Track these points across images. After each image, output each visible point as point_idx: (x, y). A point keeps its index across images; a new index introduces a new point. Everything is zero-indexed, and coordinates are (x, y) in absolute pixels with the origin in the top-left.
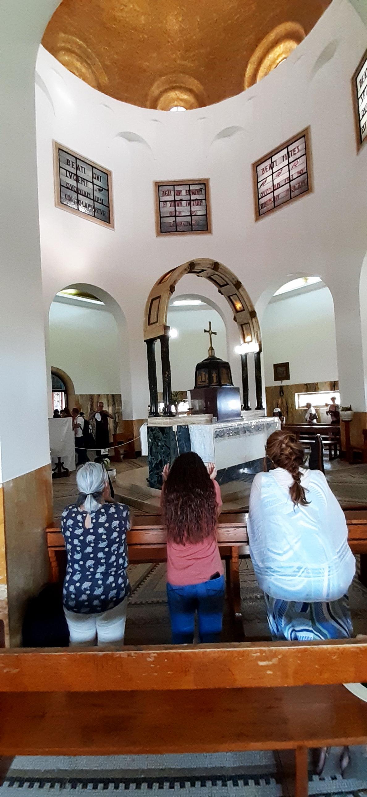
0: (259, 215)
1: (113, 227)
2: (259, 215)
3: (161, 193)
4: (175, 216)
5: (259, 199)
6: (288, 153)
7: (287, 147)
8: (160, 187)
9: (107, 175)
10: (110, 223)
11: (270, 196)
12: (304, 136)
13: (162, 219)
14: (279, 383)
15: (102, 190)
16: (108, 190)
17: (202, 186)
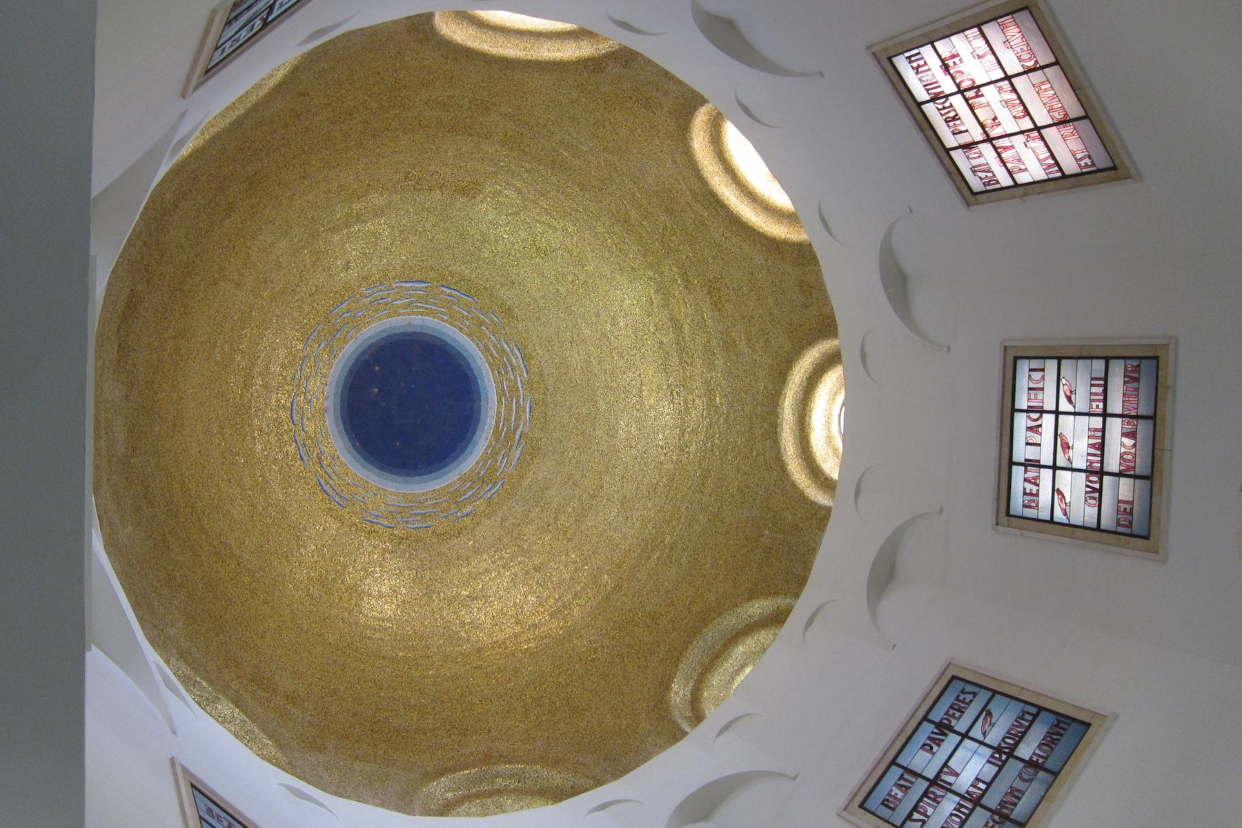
1: (1103, 717)
2: (1114, 168)
3: (1029, 513)
4: (1101, 473)
5: (1064, 176)
6: (933, 100)
7: (919, 105)
8: (1012, 512)
9: (954, 678)
10: (1088, 725)
11: (1052, 134)
12: (890, 59)
13: (1103, 527)
15: (989, 714)
16: (995, 692)
17: (1023, 367)
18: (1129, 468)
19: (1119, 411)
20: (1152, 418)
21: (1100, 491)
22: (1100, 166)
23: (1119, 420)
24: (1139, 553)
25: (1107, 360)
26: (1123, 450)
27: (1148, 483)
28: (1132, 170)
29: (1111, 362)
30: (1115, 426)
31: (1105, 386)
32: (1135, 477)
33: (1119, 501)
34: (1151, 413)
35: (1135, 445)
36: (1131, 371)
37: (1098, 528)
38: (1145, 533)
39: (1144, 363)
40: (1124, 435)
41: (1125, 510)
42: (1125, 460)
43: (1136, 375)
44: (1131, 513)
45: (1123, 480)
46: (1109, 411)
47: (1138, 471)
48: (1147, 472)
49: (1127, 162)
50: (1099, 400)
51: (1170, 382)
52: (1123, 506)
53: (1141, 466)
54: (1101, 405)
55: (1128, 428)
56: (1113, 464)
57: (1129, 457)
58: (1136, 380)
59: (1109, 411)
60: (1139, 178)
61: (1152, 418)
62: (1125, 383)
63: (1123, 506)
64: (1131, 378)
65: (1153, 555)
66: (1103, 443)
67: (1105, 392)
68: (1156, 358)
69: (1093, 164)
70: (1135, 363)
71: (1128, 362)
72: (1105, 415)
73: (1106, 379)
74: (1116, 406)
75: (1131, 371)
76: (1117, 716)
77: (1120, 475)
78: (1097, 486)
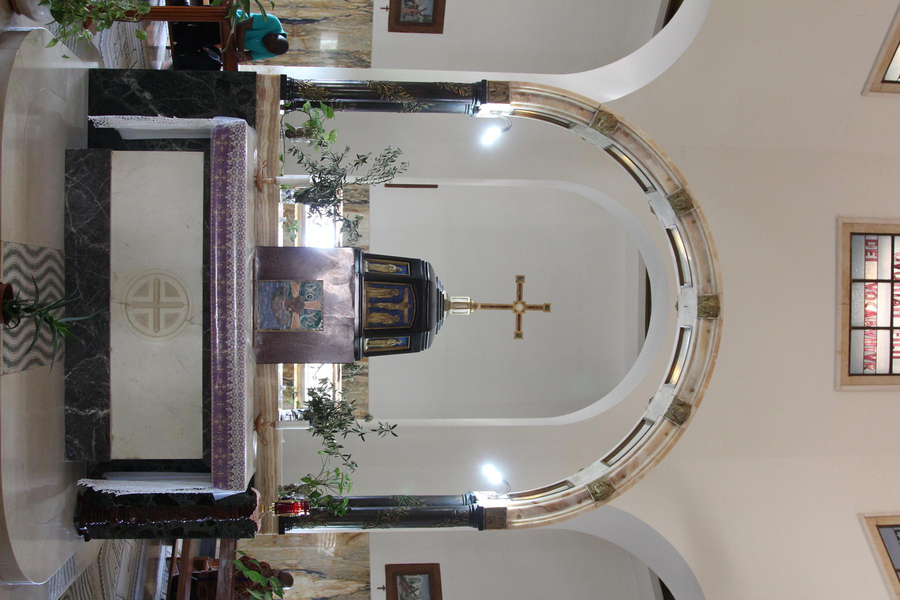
0: (879, 527)
1: (871, 91)
2: (879, 527)
13: (890, 238)
14: (378, 579)
18: (870, 287)
19: (879, 331)
20: (852, 328)
21: (893, 266)
22: (891, 530)
23: (879, 325)
24: (859, 221)
25: (891, 373)
26: (875, 301)
27: (854, 277)
28: (864, 522)
29: (887, 371)
30: (883, 320)
31: (892, 352)
32: (865, 281)
33: (877, 260)
34: (853, 332)
35: (866, 306)
36: (870, 364)
37: (893, 236)
38: (854, 237)
39: (861, 372)
40: (875, 314)
41: (871, 253)
42: (873, 293)
43: (866, 361)
44: (866, 252)
45: (875, 278)
46: (888, 332)
47: (861, 285)
48: (854, 285)
49: (868, 530)
50: (897, 340)
51: (839, 357)
52: (873, 256)
53: (859, 289)
54: (895, 336)
55: (871, 319)
56: (884, 290)
57: (870, 296)
58: (865, 357)
59: (888, 332)
60: (859, 515)
61: (852, 328)
62: (875, 355)
63: (873, 256)
64: (870, 359)
65: (846, 221)
66: (892, 305)
67: (892, 347)
68: (850, 375)
69: (896, 532)
70: (867, 371)
71: (873, 372)
72: (891, 328)
73: (891, 358)
74: (883, 337)
75: (870, 364)
76: (862, 93)
77: (877, 281)
78: (896, 270)
